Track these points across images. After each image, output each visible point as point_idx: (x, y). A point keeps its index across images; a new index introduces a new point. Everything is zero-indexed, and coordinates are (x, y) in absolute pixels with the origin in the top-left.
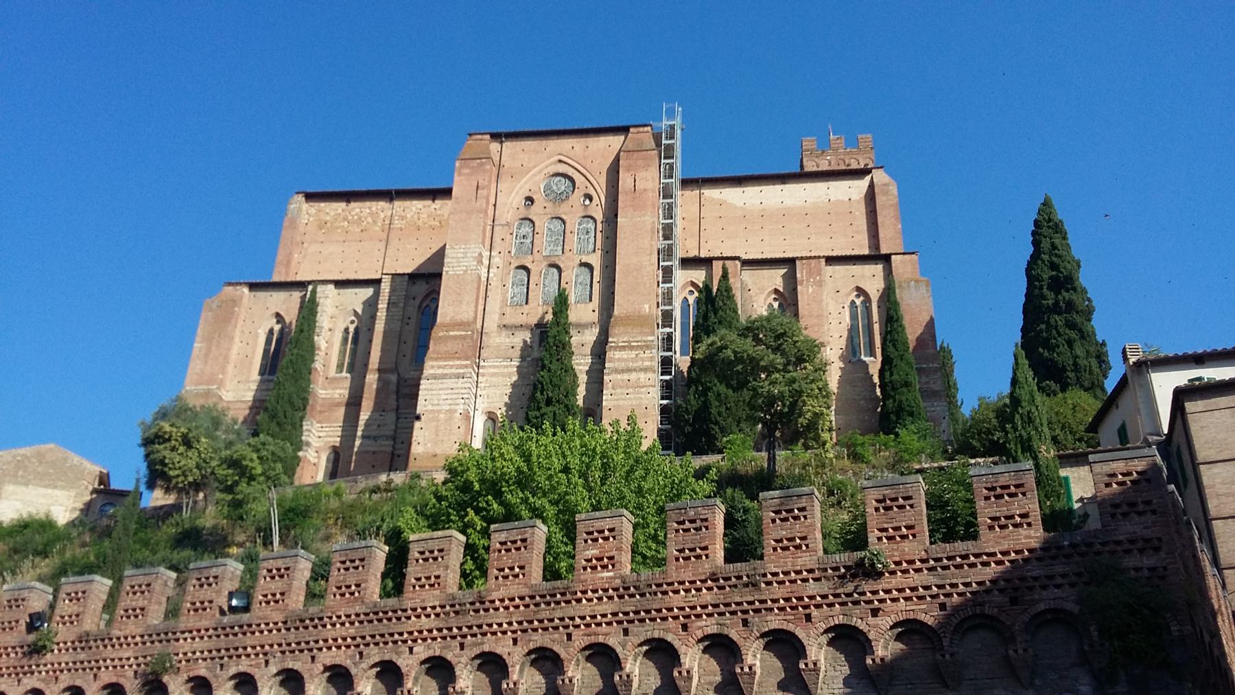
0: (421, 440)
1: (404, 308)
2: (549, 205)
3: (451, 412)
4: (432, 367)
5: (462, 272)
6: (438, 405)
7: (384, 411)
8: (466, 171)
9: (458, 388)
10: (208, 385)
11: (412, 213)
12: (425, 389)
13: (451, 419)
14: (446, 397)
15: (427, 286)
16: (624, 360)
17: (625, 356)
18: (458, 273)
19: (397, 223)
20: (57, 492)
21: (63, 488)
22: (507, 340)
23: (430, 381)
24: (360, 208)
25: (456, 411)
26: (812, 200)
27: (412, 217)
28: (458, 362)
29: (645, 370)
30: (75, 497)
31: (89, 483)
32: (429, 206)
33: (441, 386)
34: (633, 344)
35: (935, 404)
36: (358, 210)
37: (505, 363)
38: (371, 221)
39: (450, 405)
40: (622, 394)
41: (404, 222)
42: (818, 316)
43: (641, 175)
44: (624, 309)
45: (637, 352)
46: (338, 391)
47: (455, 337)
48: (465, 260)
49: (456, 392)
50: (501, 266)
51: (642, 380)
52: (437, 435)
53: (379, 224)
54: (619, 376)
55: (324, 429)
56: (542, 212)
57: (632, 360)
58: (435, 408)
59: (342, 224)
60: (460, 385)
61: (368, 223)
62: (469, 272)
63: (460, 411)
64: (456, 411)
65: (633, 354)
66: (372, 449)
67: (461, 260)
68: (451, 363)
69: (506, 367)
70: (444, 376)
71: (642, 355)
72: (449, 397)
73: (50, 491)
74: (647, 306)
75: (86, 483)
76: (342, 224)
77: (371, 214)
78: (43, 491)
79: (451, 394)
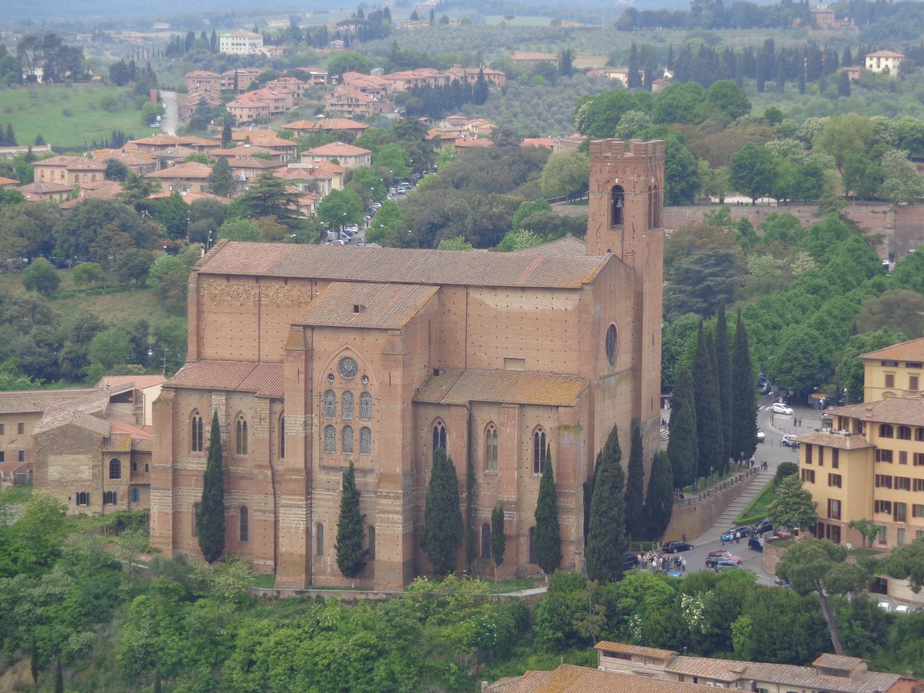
1: (270, 422)
2: (344, 382)
16: (387, 505)
19: (264, 301)
20: (81, 457)
21: (83, 453)
29: (397, 513)
43: (394, 373)
47: (295, 480)
65: (390, 501)
66: (263, 518)
70: (291, 506)
73: (76, 456)
78: (71, 457)
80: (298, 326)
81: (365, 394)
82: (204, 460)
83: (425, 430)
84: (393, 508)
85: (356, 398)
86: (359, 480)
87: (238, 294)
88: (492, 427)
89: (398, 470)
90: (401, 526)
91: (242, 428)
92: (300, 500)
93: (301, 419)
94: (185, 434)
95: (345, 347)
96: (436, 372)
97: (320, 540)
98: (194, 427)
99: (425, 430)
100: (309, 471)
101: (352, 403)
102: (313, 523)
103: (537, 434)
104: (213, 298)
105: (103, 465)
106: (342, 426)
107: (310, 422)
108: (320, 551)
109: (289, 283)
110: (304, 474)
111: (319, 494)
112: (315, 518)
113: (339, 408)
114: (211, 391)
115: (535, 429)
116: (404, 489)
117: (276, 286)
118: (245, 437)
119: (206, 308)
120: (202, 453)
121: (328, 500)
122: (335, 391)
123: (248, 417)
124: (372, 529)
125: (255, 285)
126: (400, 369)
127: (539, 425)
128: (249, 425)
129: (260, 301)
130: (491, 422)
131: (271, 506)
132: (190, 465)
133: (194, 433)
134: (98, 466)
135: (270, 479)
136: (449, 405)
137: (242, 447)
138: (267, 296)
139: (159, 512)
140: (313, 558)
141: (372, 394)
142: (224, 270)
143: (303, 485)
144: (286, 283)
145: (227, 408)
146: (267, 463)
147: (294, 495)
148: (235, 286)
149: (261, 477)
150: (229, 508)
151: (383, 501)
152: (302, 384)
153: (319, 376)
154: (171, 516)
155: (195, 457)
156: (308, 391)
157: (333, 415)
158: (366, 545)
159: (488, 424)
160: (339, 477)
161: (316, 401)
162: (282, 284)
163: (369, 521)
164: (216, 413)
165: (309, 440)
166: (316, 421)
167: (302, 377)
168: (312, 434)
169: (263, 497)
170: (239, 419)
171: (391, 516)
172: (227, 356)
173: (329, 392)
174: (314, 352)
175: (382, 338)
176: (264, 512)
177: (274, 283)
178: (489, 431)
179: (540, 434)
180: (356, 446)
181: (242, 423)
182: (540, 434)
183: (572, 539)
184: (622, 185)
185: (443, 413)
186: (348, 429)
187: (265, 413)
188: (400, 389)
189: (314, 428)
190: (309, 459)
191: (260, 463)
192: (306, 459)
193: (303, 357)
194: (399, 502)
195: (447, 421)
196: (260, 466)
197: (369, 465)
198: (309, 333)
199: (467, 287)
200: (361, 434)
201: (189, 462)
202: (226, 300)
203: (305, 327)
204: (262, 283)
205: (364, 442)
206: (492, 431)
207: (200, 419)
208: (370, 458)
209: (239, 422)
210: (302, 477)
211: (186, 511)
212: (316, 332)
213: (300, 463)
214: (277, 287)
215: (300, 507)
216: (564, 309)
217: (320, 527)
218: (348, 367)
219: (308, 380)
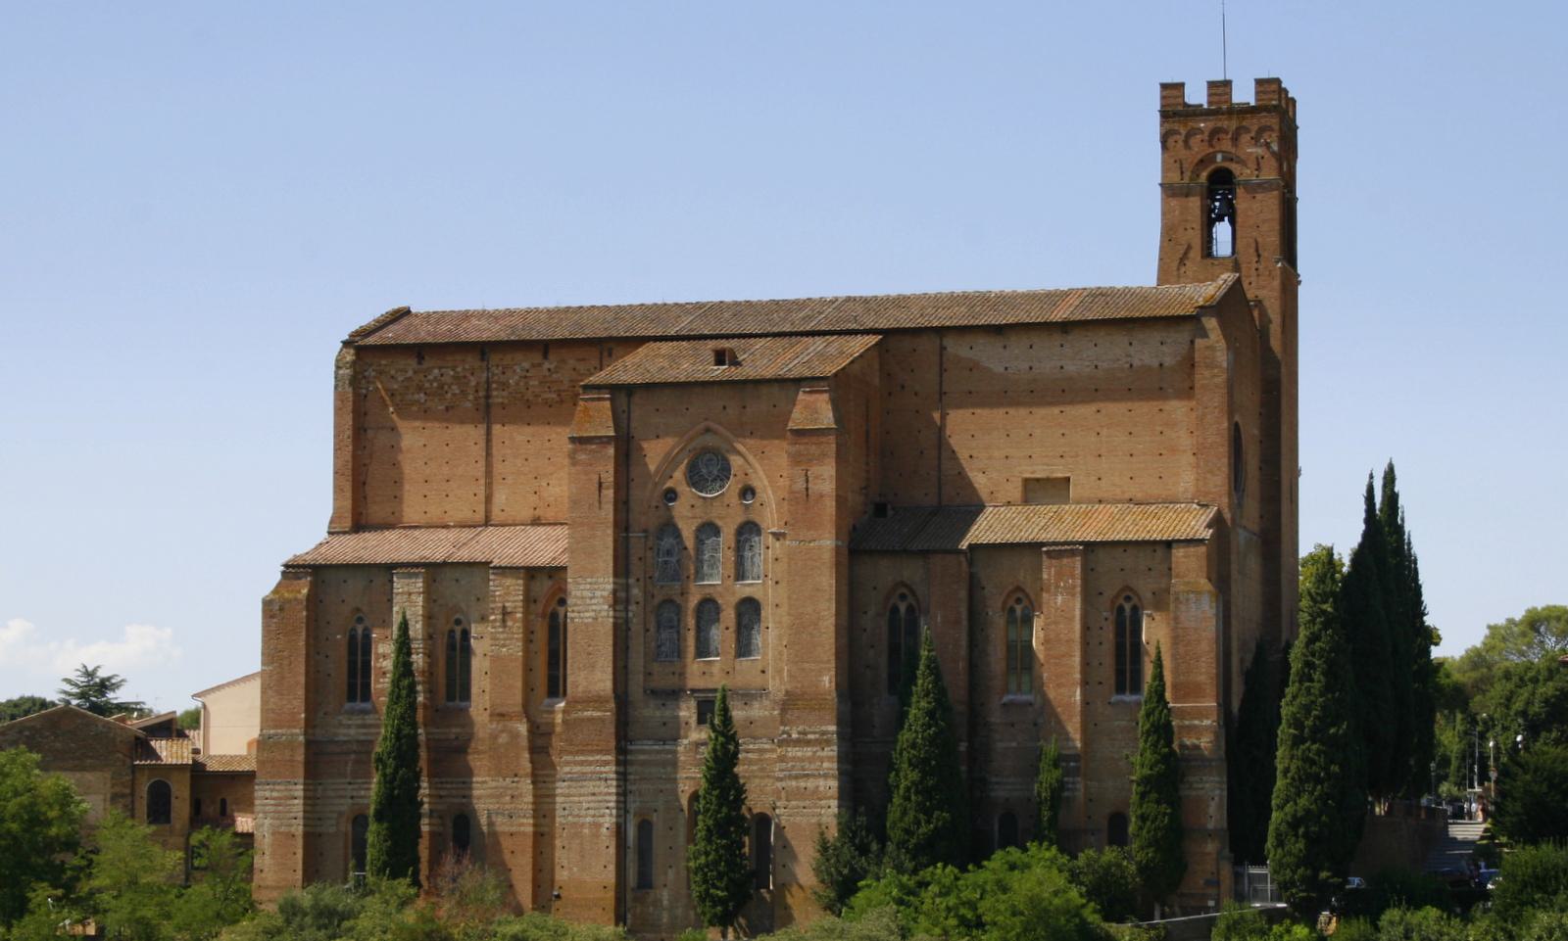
0: (565, 863)
2: (698, 503)
4: (568, 763)
5: (590, 620)
6: (578, 816)
7: (516, 775)
8: (582, 457)
9: (600, 794)
10: (289, 727)
11: (517, 377)
12: (563, 795)
13: (597, 835)
14: (588, 805)
15: (550, 583)
16: (801, 760)
17: (799, 754)
18: (586, 621)
20: (89, 776)
21: (92, 769)
22: (658, 714)
23: (566, 784)
24: (440, 368)
25: (600, 825)
26: (1105, 365)
27: (517, 384)
28: (598, 757)
29: (825, 776)
30: (112, 778)
31: (125, 755)
32: (540, 365)
33: (582, 791)
34: (811, 737)
35: (1204, 778)
36: (436, 371)
37: (657, 747)
38: (457, 392)
39: (594, 816)
40: (798, 807)
41: (505, 393)
42: (1067, 641)
44: (798, 682)
45: (815, 749)
46: (454, 730)
47: (591, 719)
48: (593, 601)
49: (600, 798)
50: (642, 604)
51: (821, 789)
52: (583, 856)
53: (471, 397)
54: (794, 783)
55: (444, 786)
56: (690, 515)
57: (811, 760)
58: (576, 820)
59: (416, 396)
61: (454, 395)
62: (600, 619)
63: (607, 825)
64: (600, 825)
65: (808, 751)
67: (588, 601)
68: (591, 758)
70: (582, 778)
71: (818, 754)
72: (592, 805)
74: (826, 679)
75: (120, 755)
76: (416, 396)
77: (456, 378)
79: (595, 802)
86: (738, 714)
87: (441, 387)
88: (1018, 601)
90: (834, 803)
93: (606, 585)
95: (702, 426)
103: (1121, 609)
105: (132, 794)
109: (551, 357)
110: (612, 705)
112: (633, 805)
115: (1117, 597)
116: (839, 724)
117: (523, 362)
125: (477, 364)
127: (1128, 588)
129: (488, 397)
130: (1019, 589)
132: (345, 731)
133: (352, 665)
134: (123, 796)
135: (524, 743)
138: (504, 385)
139: (273, 834)
140: (629, 896)
144: (545, 356)
146: (519, 708)
147: (592, 752)
149: (503, 739)
152: (608, 511)
154: (300, 842)
155: (352, 712)
159: (1009, 595)
161: (637, 549)
162: (537, 357)
166: (636, 592)
167: (609, 494)
168: (627, 621)
171: (810, 784)
177: (519, 356)
178: (1012, 610)
179: (1127, 607)
182: (1127, 607)
183: (1211, 826)
189: (633, 607)
194: (832, 751)
196: (502, 715)
199: (941, 331)
201: (341, 725)
202: (418, 401)
204: (495, 358)
206: (1019, 609)
209: (452, 631)
210: (607, 713)
211: (332, 830)
212: (637, 399)
214: (526, 365)
216: (1156, 364)
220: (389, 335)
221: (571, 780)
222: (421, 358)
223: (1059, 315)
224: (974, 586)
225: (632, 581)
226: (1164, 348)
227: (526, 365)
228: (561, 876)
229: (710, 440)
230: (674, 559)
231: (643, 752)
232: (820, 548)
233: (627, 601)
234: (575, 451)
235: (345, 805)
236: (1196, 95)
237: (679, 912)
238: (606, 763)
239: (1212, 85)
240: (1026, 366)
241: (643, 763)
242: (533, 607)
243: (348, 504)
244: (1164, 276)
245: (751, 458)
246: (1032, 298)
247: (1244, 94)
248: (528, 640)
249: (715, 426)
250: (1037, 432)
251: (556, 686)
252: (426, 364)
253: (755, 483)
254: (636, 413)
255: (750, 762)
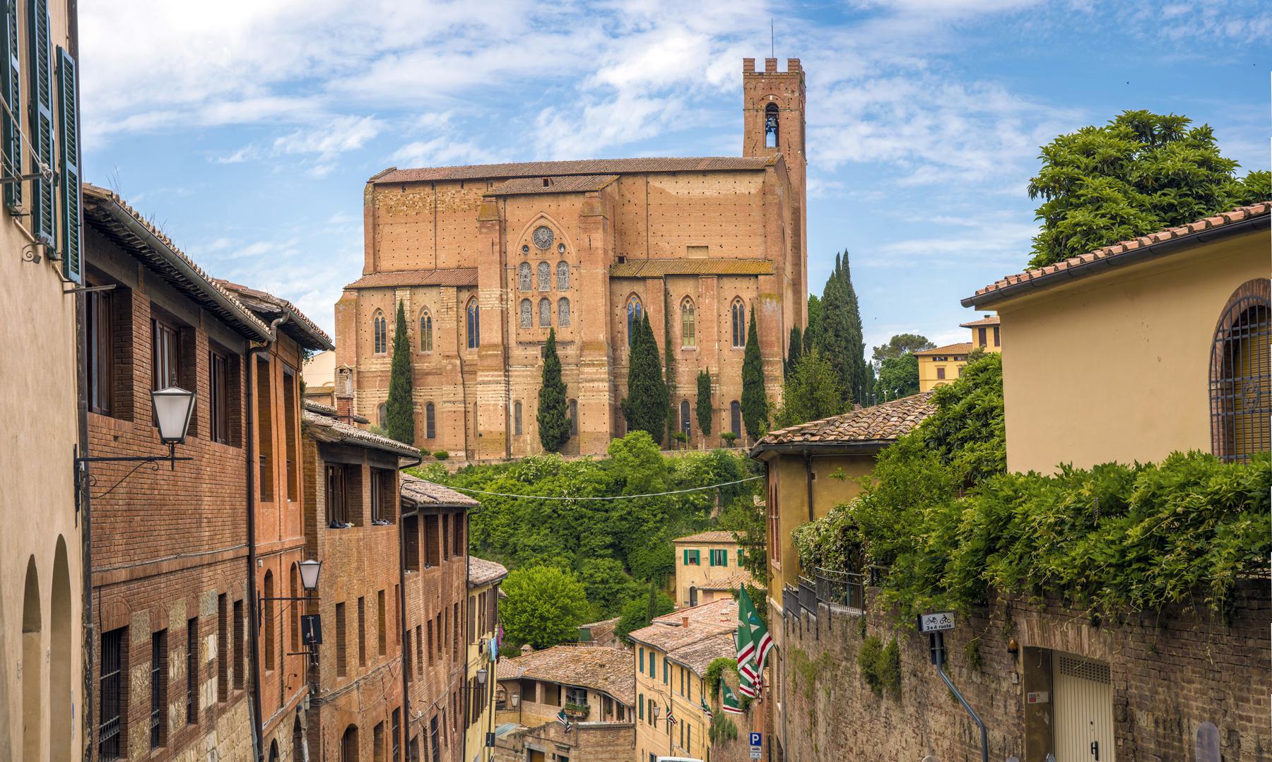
0: (482, 423)
1: (457, 311)
3: (497, 405)
4: (481, 376)
13: (496, 409)
15: (469, 293)
16: (590, 373)
25: (498, 405)
29: (602, 380)
43: (594, 236)
47: (491, 355)
60: (499, 388)
66: (452, 409)
69: (523, 371)
70: (489, 382)
74: (601, 335)
80: (490, 196)
81: (563, 262)
82: (389, 360)
83: (620, 306)
84: (598, 376)
85: (553, 268)
86: (560, 352)
89: (602, 337)
90: (607, 394)
91: (427, 325)
92: (499, 376)
93: (497, 291)
94: (368, 335)
96: (621, 260)
97: (518, 420)
98: (377, 327)
99: (620, 306)
100: (506, 349)
101: (548, 274)
102: (511, 401)
104: (389, 209)
106: (540, 298)
107: (505, 297)
108: (518, 431)
110: (502, 348)
111: (516, 370)
112: (513, 396)
113: (534, 281)
114: (394, 288)
118: (430, 335)
119: (381, 221)
120: (385, 354)
121: (526, 377)
122: (531, 262)
123: (433, 314)
124: (574, 402)
126: (601, 231)
128: (433, 321)
131: (460, 397)
133: (377, 333)
135: (460, 370)
136: (644, 279)
137: (426, 345)
140: (512, 438)
141: (570, 263)
142: (398, 180)
143: (501, 359)
145: (411, 303)
146: (456, 353)
147: (492, 370)
148: (412, 195)
149: (449, 367)
150: (416, 404)
151: (586, 370)
153: (514, 249)
156: (504, 265)
157: (529, 288)
158: (568, 415)
160: (536, 352)
161: (511, 275)
163: (570, 394)
164: (402, 305)
165: (505, 315)
166: (511, 295)
167: (497, 248)
168: (507, 309)
169: (452, 387)
170: (423, 315)
171: (596, 384)
172: (403, 267)
173: (525, 263)
174: (508, 224)
175: (578, 203)
176: (454, 403)
180: (555, 317)
181: (426, 320)
184: (777, 102)
185: (638, 288)
186: (546, 301)
187: (453, 303)
188: (600, 252)
189: (510, 303)
190: (505, 336)
191: (447, 354)
192: (502, 334)
193: (497, 227)
194: (605, 369)
195: (643, 296)
197: (569, 337)
198: (501, 204)
200: (560, 306)
203: (498, 197)
205: (562, 314)
207: (383, 321)
208: (570, 330)
209: (423, 318)
212: (508, 201)
213: (496, 338)
215: (498, 383)
217: (518, 404)
218: (543, 236)
219: (503, 253)
220: (388, 179)
221: (484, 383)
222: (404, 190)
223: (700, 167)
224: (667, 293)
225: (509, 290)
226: (750, 185)
227: (454, 192)
228: (481, 428)
229: (543, 222)
230: (528, 280)
231: (517, 371)
232: (597, 273)
233: (507, 300)
234: (481, 227)
235: (377, 402)
236: (760, 67)
237: (535, 445)
238: (500, 376)
239: (768, 61)
240: (687, 192)
241: (518, 376)
242: (461, 305)
243: (371, 261)
244: (745, 153)
245: (563, 232)
246: (687, 161)
247: (782, 68)
248: (458, 321)
249: (546, 215)
250: (693, 224)
251: (473, 342)
252: (406, 192)
253: (565, 243)
254: (508, 209)
255: (567, 375)
